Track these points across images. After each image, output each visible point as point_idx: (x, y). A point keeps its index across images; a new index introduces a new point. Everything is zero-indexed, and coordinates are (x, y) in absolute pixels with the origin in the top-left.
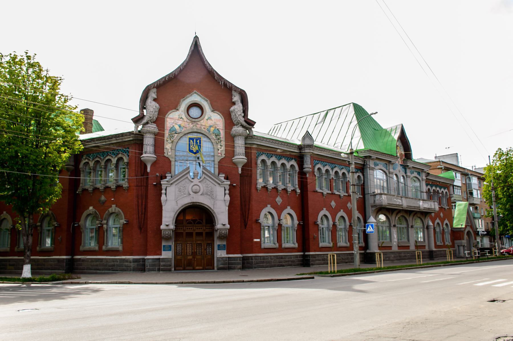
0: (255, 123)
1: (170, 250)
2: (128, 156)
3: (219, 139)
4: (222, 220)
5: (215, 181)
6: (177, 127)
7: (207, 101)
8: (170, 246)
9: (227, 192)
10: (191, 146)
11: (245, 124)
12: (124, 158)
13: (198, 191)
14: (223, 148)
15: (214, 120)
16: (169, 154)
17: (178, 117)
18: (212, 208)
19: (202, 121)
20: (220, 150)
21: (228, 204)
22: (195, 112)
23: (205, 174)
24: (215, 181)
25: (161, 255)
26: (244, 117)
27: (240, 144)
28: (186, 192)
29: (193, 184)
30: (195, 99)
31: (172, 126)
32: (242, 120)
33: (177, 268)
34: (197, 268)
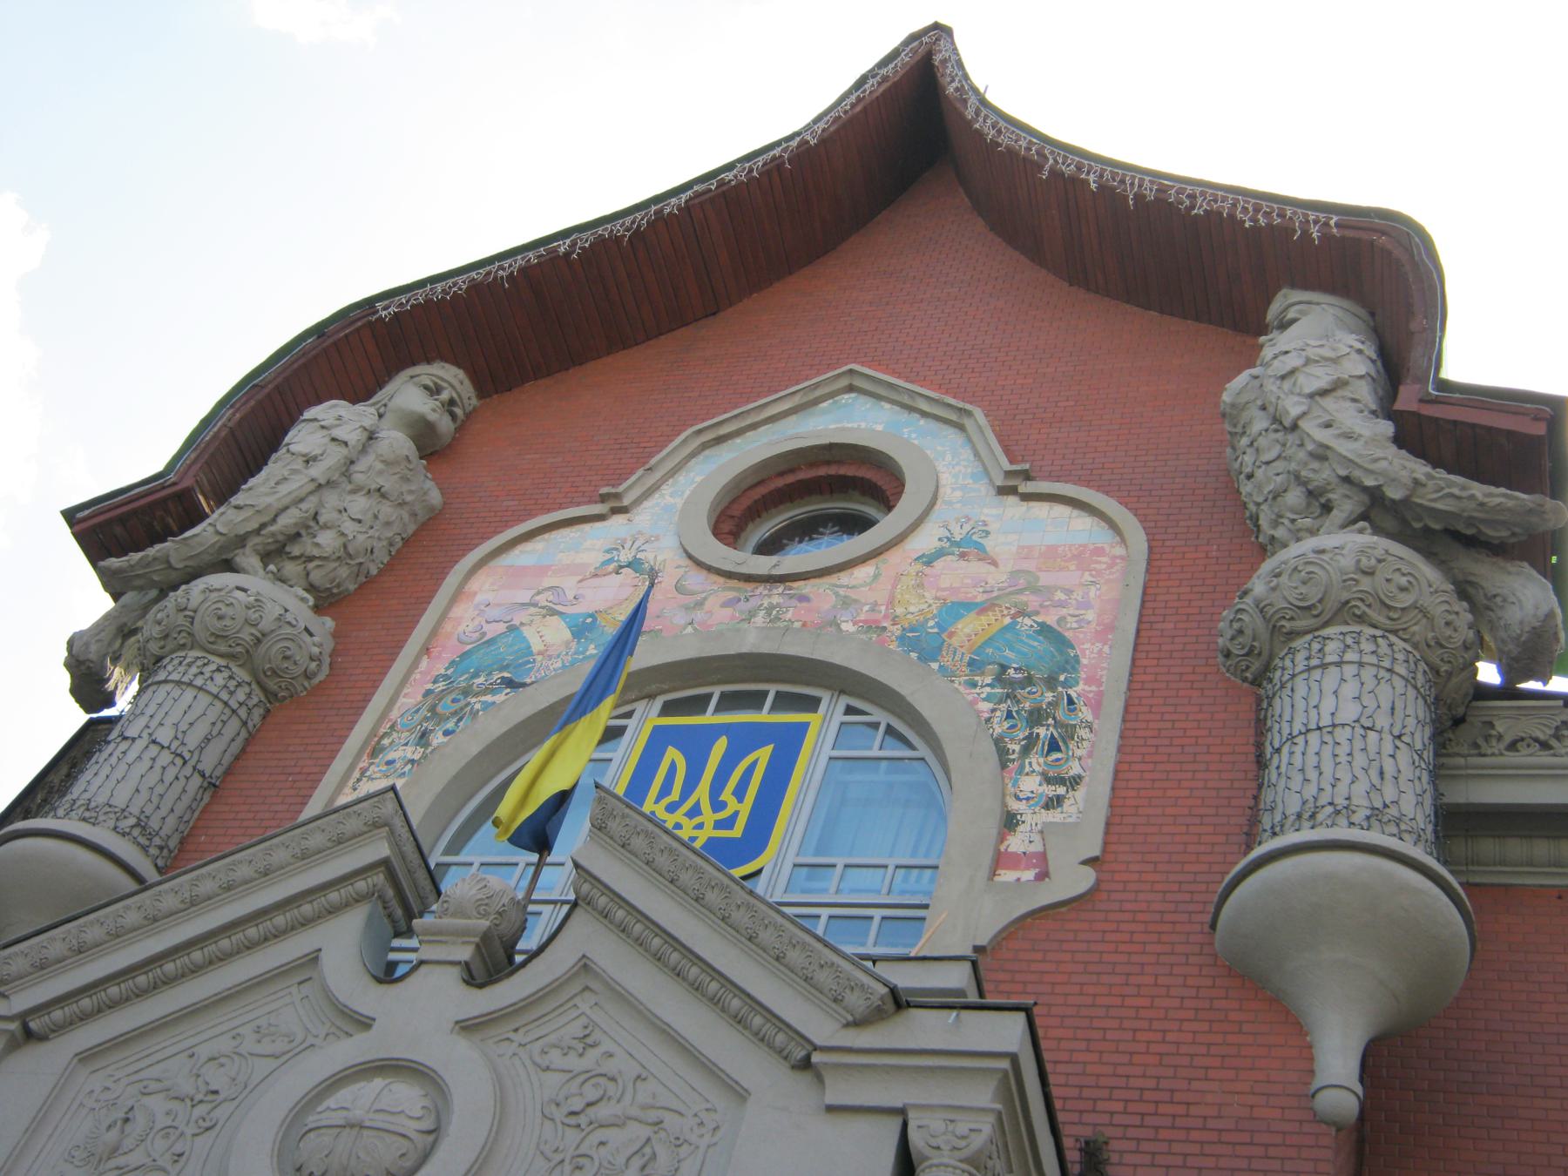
11: (1402, 471)
14: (1086, 810)
19: (864, 572)
24: (745, 1014)
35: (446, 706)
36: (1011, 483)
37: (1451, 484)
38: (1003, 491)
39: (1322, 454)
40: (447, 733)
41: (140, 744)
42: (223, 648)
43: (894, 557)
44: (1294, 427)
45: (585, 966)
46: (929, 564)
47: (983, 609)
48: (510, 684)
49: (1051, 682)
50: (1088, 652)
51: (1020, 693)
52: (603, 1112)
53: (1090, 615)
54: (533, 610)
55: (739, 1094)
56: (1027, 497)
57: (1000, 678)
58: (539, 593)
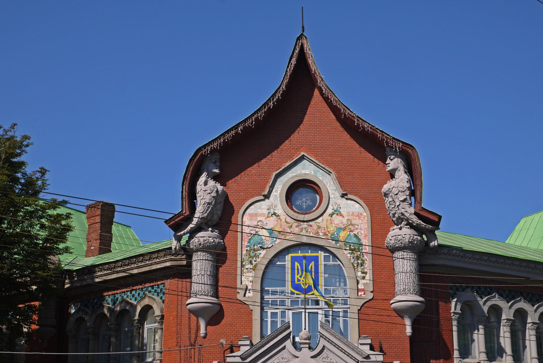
2: (163, 302)
3: (358, 258)
5: (349, 355)
7: (329, 173)
10: (296, 276)
11: (415, 220)
12: (155, 306)
15: (344, 215)
16: (248, 294)
17: (266, 212)
20: (362, 282)
22: (303, 198)
27: (404, 267)
30: (304, 172)
35: (252, 254)
40: (255, 261)
41: (206, 276)
43: (325, 215)
46: (331, 217)
47: (344, 229)
48: (262, 248)
53: (363, 232)
57: (350, 249)
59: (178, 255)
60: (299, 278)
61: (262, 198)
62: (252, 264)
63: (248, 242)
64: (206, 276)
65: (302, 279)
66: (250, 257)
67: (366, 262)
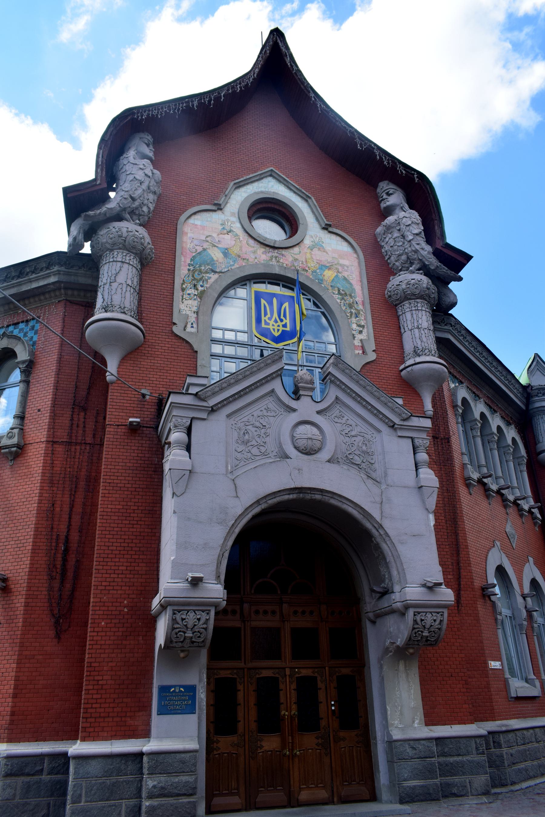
0: (468, 258)
1: (191, 710)
3: (351, 306)
4: (416, 566)
6: (216, 255)
7: (305, 199)
8: (192, 689)
9: (423, 456)
11: (433, 262)
13: (318, 444)
16: (189, 329)
18: (376, 515)
19: (296, 249)
20: (359, 337)
21: (432, 502)
23: (341, 385)
24: (378, 414)
25: (146, 734)
26: (429, 240)
28: (271, 447)
29: (294, 418)
31: (199, 249)
32: (425, 250)
33: (217, 801)
34: (304, 796)
35: (196, 276)
36: (326, 227)
37: (444, 269)
38: (324, 228)
39: (416, 251)
40: (202, 286)
42: (134, 251)
44: (410, 241)
45: (337, 398)
46: (312, 250)
47: (329, 268)
49: (351, 296)
50: (357, 288)
51: (345, 298)
52: (353, 433)
53: (354, 276)
54: (208, 243)
55: (379, 431)
56: (330, 232)
57: (339, 293)
58: (207, 237)
59: (72, 267)
60: (268, 321)
61: (214, 208)
62: (197, 289)
63: (191, 260)
64: (125, 286)
65: (272, 322)
66: (195, 279)
67: (361, 312)
